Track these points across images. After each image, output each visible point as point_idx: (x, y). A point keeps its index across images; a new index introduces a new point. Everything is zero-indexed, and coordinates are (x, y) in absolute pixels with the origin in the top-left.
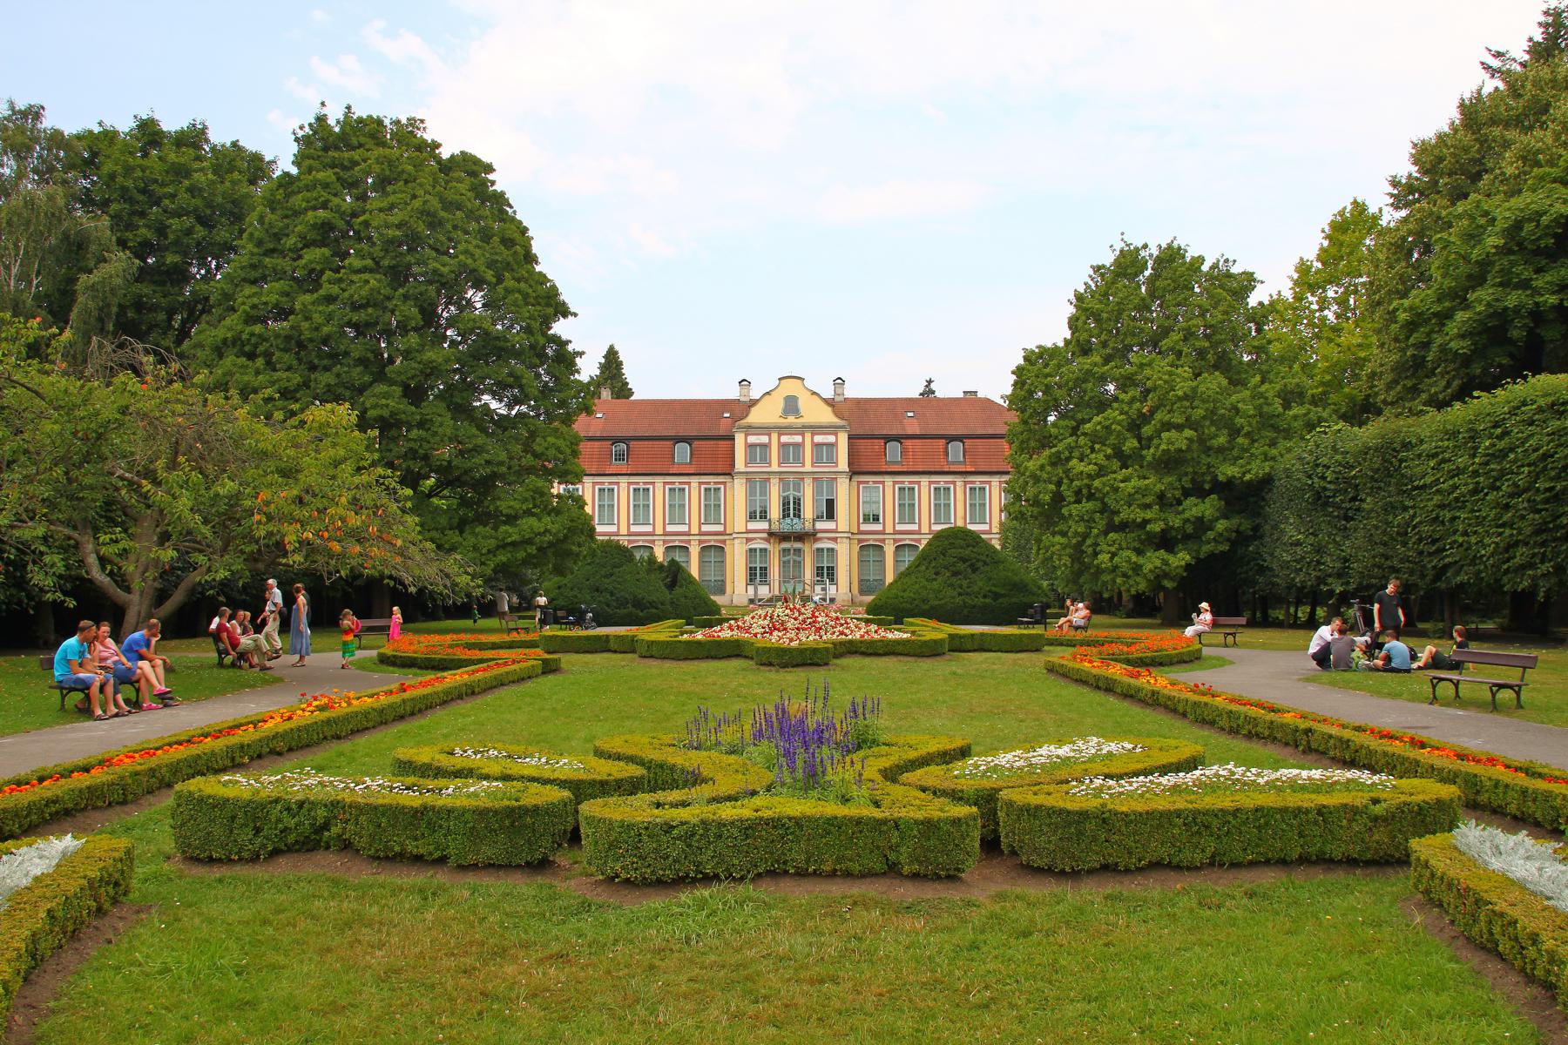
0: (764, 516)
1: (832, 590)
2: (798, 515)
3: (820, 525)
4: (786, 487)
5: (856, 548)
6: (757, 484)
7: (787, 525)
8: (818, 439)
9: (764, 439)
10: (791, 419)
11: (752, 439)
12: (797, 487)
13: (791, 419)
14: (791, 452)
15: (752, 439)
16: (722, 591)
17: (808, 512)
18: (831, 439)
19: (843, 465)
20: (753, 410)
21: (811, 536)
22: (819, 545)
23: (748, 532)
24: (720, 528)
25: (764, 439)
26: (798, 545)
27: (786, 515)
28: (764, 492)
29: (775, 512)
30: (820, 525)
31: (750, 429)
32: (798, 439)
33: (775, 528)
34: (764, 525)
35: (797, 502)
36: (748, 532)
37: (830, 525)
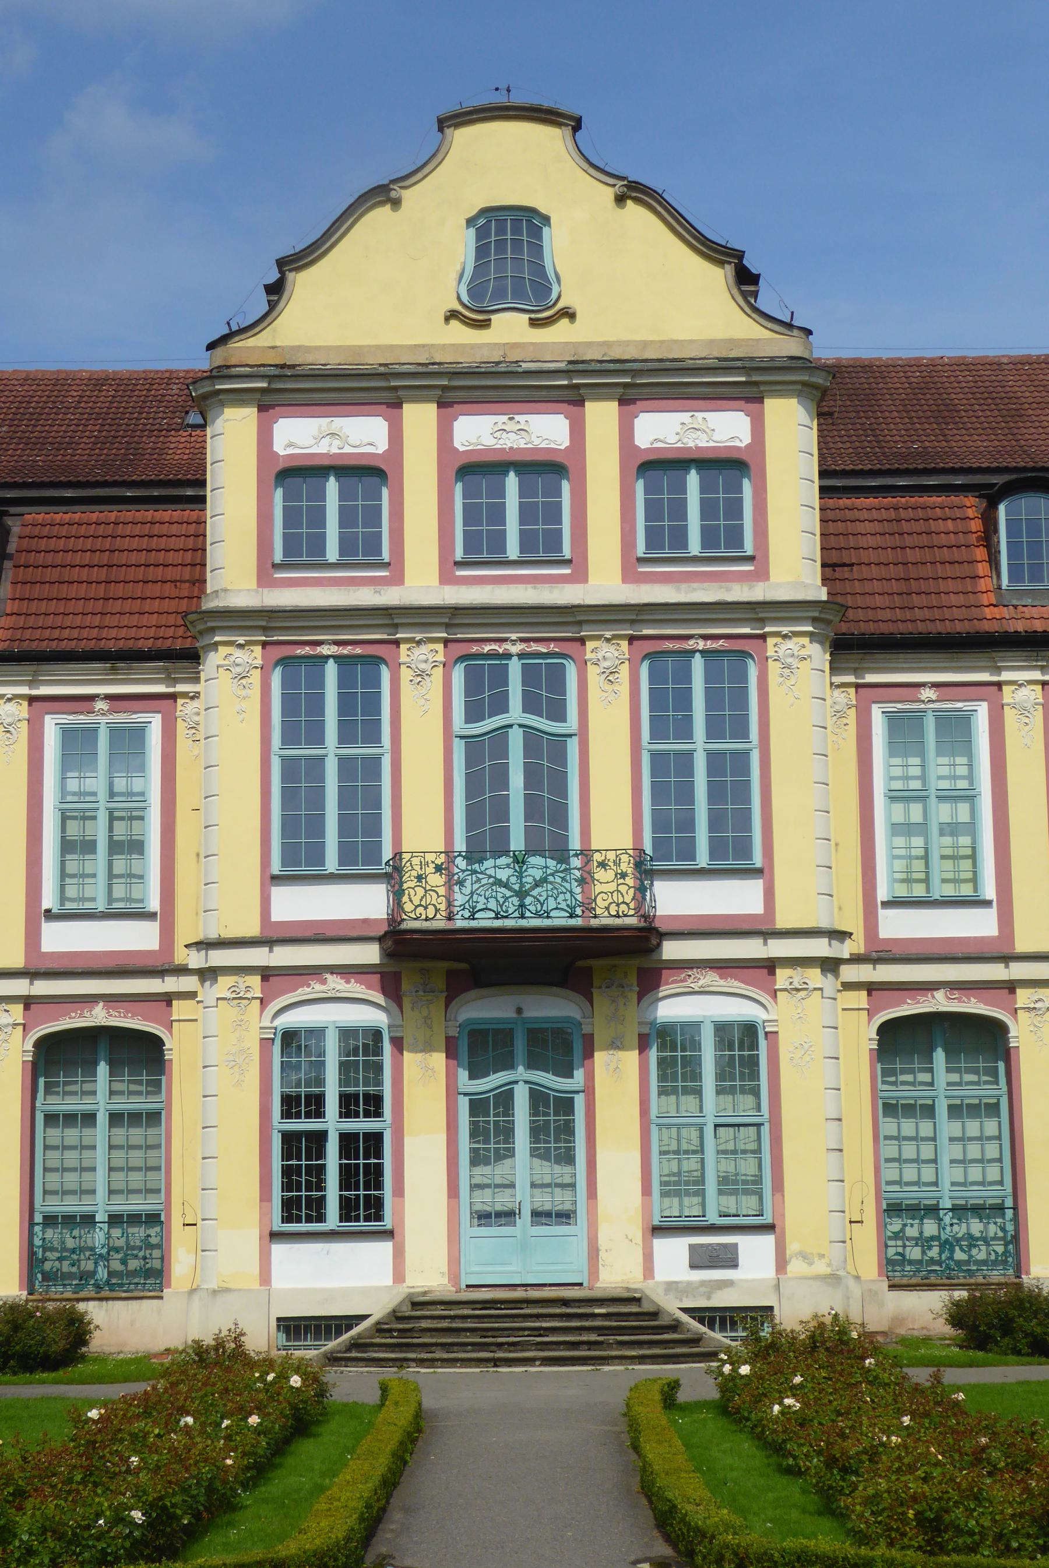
0: (366, 856)
1: (754, 1272)
2: (551, 835)
3: (675, 899)
4: (484, 692)
5: (867, 1035)
6: (330, 667)
7: (483, 904)
8: (660, 429)
9: (362, 434)
10: (510, 331)
11: (300, 435)
12: (547, 692)
13: (510, 331)
14: (511, 503)
15: (300, 435)
16: (147, 1277)
17: (610, 811)
18: (725, 428)
19: (792, 558)
20: (304, 284)
21: (619, 960)
22: (672, 1008)
23: (273, 937)
24: (139, 938)
25: (362, 434)
26: (550, 1007)
27: (484, 839)
28: (362, 717)
29: (424, 815)
30: (675, 899)
31: (289, 386)
32: (546, 430)
33: (427, 907)
34: (368, 903)
35: (551, 765)
36: (273, 937)
37: (739, 898)
